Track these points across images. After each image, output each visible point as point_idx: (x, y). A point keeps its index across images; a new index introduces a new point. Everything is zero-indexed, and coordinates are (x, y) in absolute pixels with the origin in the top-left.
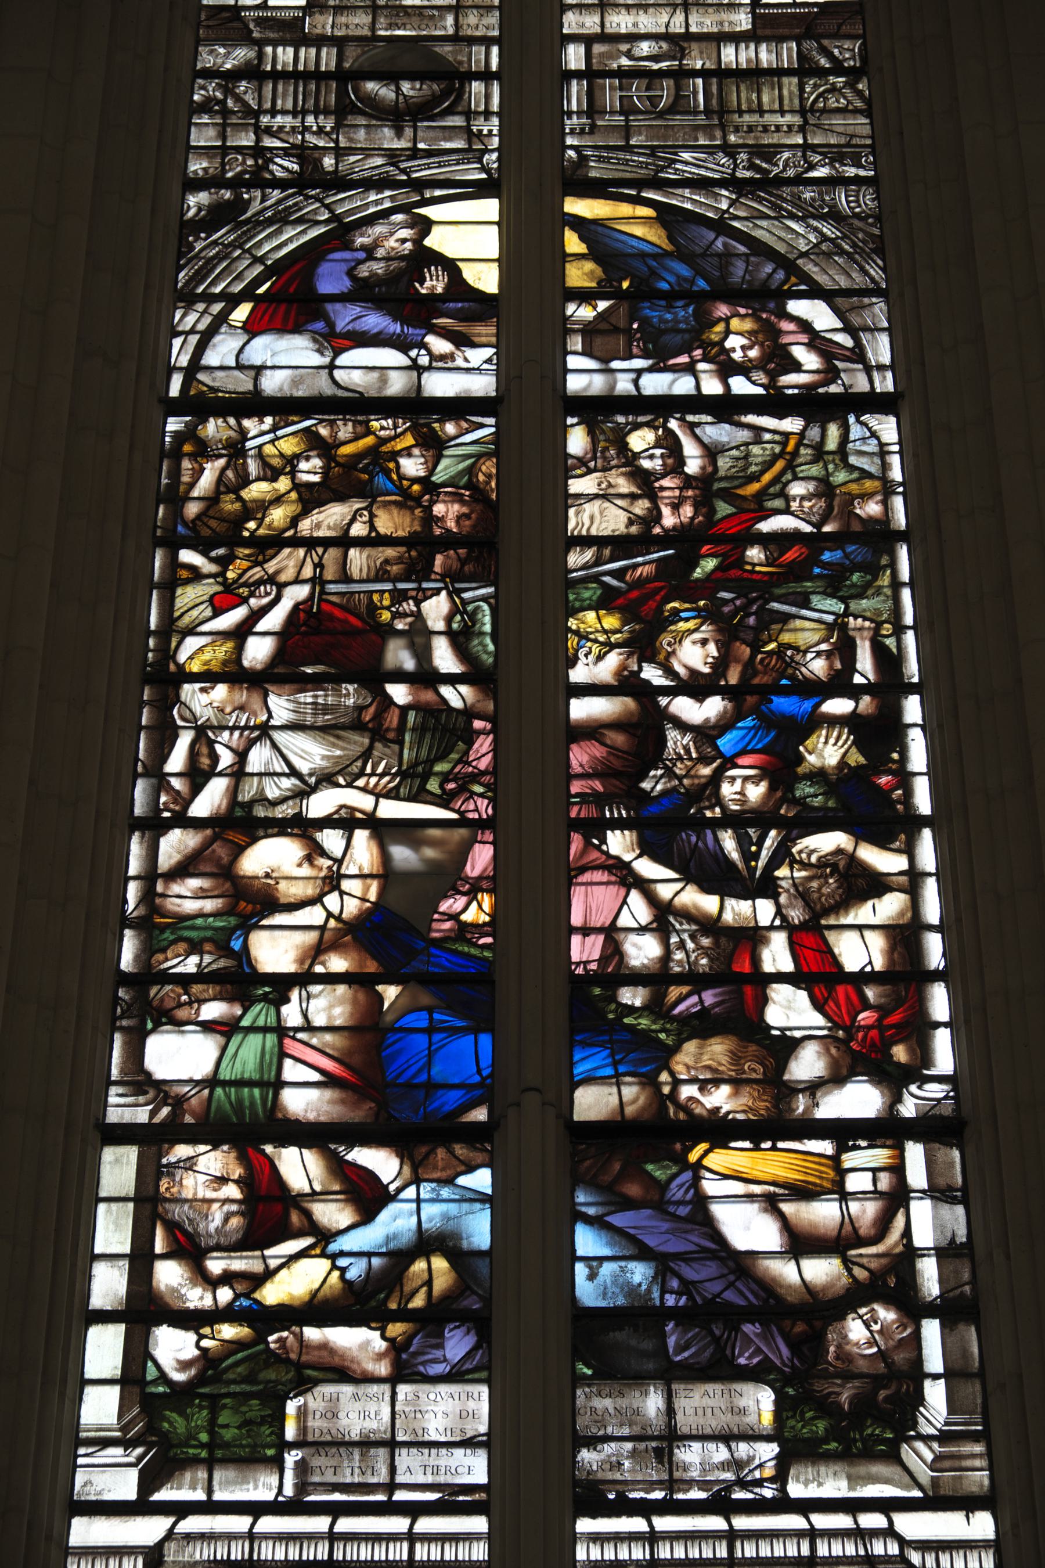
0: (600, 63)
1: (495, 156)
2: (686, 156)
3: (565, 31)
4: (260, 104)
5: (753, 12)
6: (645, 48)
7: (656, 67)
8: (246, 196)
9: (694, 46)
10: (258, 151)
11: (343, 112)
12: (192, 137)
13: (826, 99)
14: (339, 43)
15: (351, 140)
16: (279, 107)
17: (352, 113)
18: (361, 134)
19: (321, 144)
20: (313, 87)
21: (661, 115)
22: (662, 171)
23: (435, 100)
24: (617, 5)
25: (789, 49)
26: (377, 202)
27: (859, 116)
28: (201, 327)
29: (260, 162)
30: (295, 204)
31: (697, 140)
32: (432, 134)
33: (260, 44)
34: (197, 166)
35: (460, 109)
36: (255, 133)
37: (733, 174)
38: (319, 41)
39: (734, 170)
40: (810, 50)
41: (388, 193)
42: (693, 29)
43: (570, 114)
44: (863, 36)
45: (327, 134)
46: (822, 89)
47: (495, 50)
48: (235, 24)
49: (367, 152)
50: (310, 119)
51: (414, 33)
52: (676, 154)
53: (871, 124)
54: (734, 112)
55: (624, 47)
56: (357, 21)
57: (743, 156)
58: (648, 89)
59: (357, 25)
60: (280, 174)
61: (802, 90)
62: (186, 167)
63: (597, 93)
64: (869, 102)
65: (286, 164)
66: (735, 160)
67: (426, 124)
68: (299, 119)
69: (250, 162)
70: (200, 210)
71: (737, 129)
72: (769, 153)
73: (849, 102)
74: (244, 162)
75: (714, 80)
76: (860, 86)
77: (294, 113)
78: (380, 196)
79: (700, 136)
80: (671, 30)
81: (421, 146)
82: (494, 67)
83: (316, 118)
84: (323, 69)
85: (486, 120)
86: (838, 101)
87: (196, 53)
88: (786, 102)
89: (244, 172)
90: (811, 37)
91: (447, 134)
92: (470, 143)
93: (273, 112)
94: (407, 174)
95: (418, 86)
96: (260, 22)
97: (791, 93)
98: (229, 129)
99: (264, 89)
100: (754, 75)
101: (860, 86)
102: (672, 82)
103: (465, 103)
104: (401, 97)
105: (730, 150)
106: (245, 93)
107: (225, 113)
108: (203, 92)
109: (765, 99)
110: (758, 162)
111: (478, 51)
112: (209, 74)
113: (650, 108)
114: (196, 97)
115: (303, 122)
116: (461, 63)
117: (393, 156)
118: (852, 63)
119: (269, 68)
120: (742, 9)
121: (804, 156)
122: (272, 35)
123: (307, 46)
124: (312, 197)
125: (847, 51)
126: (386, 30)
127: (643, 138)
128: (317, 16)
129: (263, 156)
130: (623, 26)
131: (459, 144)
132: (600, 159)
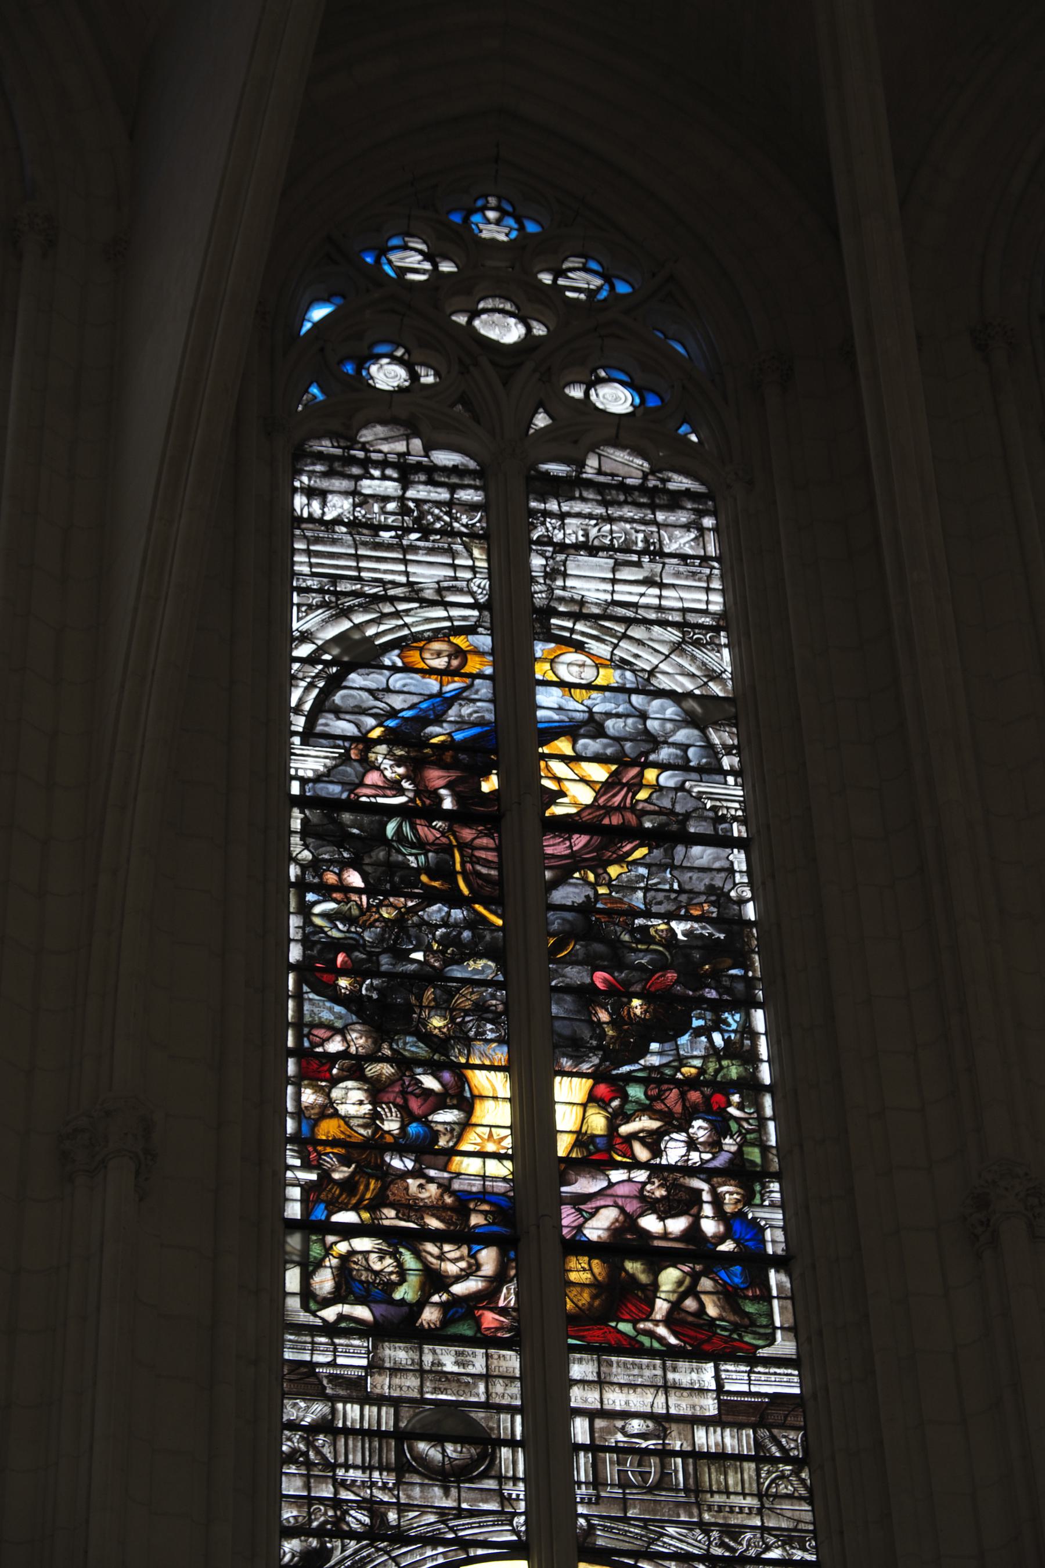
0: (601, 1437)
1: (522, 1519)
2: (671, 1530)
3: (572, 1405)
4: (335, 1458)
5: (718, 1398)
6: (636, 1425)
7: (644, 1444)
8: (329, 1545)
9: (674, 1426)
10: (336, 1503)
11: (401, 1469)
12: (284, 1486)
13: (777, 1485)
14: (395, 1402)
15: (409, 1497)
16: (350, 1462)
17: (410, 1472)
18: (417, 1491)
19: (386, 1499)
20: (376, 1444)
21: (650, 1490)
22: (652, 1543)
23: (475, 1463)
24: (612, 1384)
25: (748, 1436)
26: (433, 1558)
27: (803, 1503)
29: (339, 1513)
30: (369, 1555)
31: (679, 1516)
32: (472, 1495)
33: (332, 1400)
34: (289, 1514)
35: (493, 1473)
36: (334, 1486)
37: (708, 1550)
38: (380, 1401)
39: (709, 1546)
40: (764, 1438)
41: (441, 1550)
42: (672, 1411)
43: (579, 1483)
44: (804, 1428)
45: (391, 1490)
46: (774, 1475)
47: (518, 1419)
48: (312, 1380)
49: (423, 1509)
50: (376, 1474)
51: (454, 1398)
52: (663, 1528)
53: (813, 1511)
54: (707, 1492)
55: (619, 1424)
56: (408, 1384)
57: (715, 1534)
58: (639, 1465)
59: (409, 1387)
60: (355, 1526)
61: (758, 1476)
62: (280, 1515)
63: (600, 1466)
64: (810, 1490)
65: (359, 1516)
66: (709, 1537)
67: (467, 1485)
68: (367, 1475)
69: (330, 1513)
70: (293, 1556)
71: (710, 1509)
72: (733, 1532)
73: (795, 1489)
74: (325, 1514)
75: (691, 1461)
76: (803, 1475)
77: (363, 1468)
78: (435, 1552)
79: (681, 1512)
80: (655, 1410)
81: (464, 1506)
82: (518, 1438)
83: (381, 1474)
84: (383, 1428)
85: (514, 1485)
86: (786, 1488)
87: (282, 1406)
88: (747, 1485)
89: (326, 1522)
90: (764, 1426)
91: (484, 1496)
92: (502, 1506)
93: (347, 1467)
94: (455, 1532)
95: (459, 1449)
96: (332, 1378)
97: (750, 1477)
98: (312, 1481)
99: (338, 1443)
100: (721, 1458)
101: (803, 1475)
102: (657, 1460)
103: (496, 1468)
104: (446, 1459)
105: (705, 1528)
106: (323, 1446)
107: (309, 1464)
108: (289, 1443)
109: (731, 1481)
110: (727, 1540)
111: (505, 1418)
112: (294, 1426)
113: (641, 1483)
114: (285, 1448)
115: (370, 1478)
116: (492, 1429)
117: (443, 1513)
118: (796, 1453)
119: (340, 1425)
120: (710, 1394)
121: (762, 1537)
122: (342, 1393)
123: (371, 1405)
124: (381, 1549)
125: (792, 1440)
126: (432, 1393)
127: (636, 1511)
128: (376, 1376)
129: (341, 1508)
130: (617, 1403)
131: (493, 1506)
132: (605, 1529)
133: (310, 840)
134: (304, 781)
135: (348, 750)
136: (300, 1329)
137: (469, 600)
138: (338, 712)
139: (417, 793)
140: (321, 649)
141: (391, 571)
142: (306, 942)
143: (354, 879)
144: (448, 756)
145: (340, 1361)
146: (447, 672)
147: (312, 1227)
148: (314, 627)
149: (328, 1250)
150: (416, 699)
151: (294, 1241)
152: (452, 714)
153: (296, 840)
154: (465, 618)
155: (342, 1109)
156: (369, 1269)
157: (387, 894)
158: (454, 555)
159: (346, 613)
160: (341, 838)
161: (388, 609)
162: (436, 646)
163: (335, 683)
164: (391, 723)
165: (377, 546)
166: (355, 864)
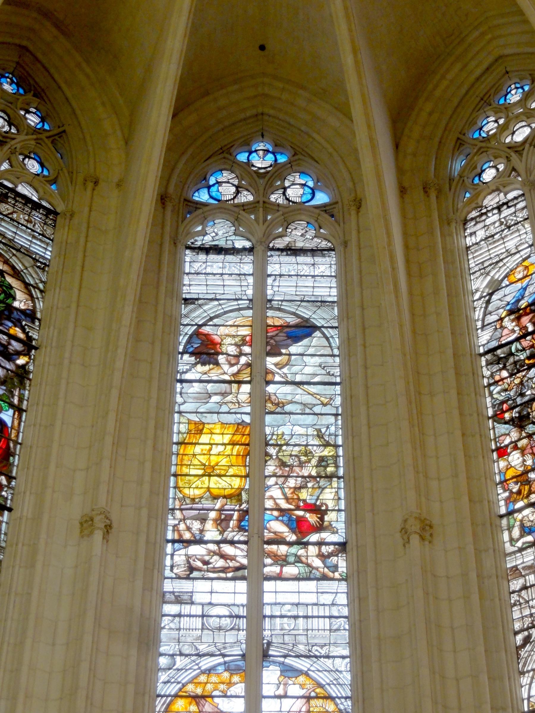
28: (528, 682)
34: (517, 626)
96: (524, 568)
107: (520, 604)
133: (489, 367)
134: (484, 345)
135: (496, 326)
136: (510, 554)
137: (527, 245)
138: (490, 313)
139: (520, 330)
140: (483, 292)
141: (499, 249)
142: (493, 406)
143: (505, 374)
144: (528, 310)
145: (525, 560)
146: (525, 277)
147: (510, 513)
148: (479, 284)
149: (515, 520)
150: (514, 294)
151: (504, 521)
152: (527, 293)
153: (484, 369)
154: (526, 253)
155: (513, 465)
156: (530, 521)
157: (515, 374)
158: (518, 230)
159: (488, 274)
160: (499, 360)
161: (501, 264)
162: (518, 269)
163: (488, 302)
164: (508, 308)
165: (494, 242)
166: (504, 368)
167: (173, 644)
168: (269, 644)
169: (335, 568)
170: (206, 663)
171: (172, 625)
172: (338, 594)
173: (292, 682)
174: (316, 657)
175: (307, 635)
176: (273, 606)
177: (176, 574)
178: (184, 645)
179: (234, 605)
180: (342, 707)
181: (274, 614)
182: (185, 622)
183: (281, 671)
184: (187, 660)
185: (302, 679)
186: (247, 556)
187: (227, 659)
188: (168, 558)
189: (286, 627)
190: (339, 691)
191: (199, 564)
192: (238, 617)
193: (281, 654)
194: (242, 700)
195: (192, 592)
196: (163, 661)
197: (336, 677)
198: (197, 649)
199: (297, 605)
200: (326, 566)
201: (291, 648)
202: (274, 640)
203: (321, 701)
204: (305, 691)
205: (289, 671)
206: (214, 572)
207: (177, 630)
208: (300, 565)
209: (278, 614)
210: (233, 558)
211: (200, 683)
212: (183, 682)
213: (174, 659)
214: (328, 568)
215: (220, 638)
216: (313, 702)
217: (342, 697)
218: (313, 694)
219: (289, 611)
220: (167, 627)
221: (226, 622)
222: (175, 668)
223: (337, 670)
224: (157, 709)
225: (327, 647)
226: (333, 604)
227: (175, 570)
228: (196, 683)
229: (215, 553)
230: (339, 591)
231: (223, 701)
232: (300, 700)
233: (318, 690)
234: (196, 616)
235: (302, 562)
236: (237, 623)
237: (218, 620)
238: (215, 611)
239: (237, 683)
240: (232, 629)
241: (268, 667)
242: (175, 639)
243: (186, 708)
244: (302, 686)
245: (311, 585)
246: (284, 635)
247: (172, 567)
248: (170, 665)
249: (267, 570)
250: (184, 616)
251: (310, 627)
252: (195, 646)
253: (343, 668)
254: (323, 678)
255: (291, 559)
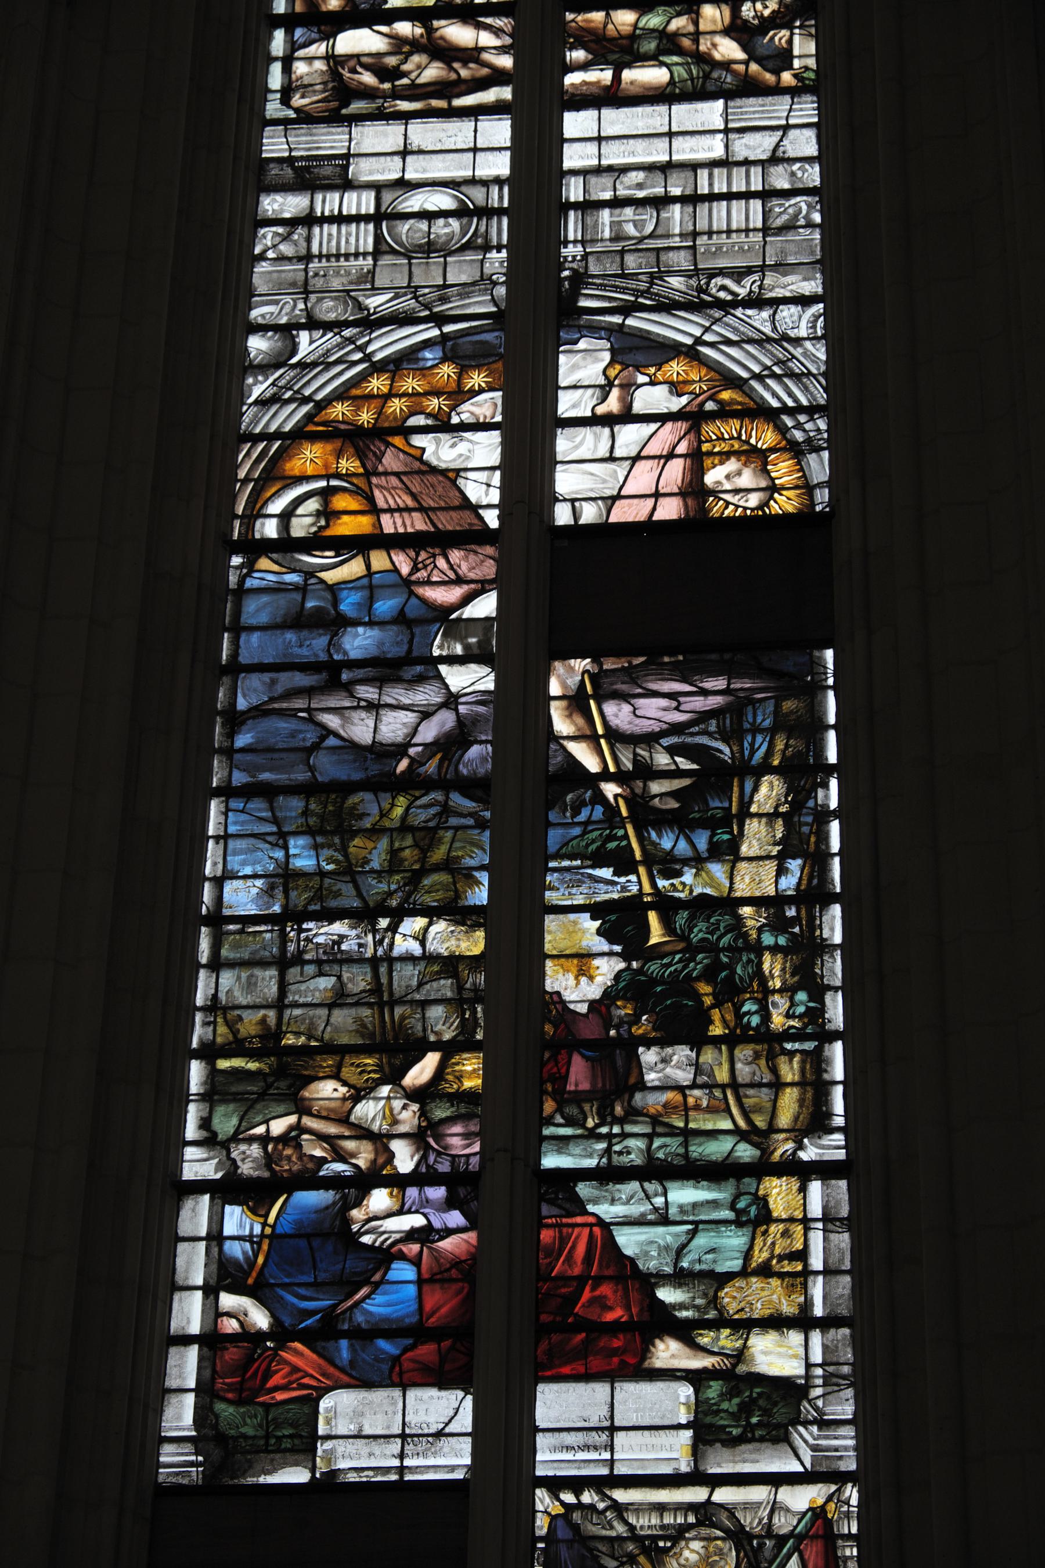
167: (288, 298)
168: (580, 279)
169: (783, 58)
170: (386, 343)
171: (286, 249)
172: (793, 134)
173: (646, 379)
174: (720, 304)
175: (693, 248)
176: (593, 180)
177: (297, 110)
178: (320, 300)
179: (473, 181)
180: (799, 435)
181: (594, 197)
182: (323, 238)
183: (612, 350)
184: (330, 339)
185: (675, 368)
186: (511, 46)
187: (448, 329)
188: (276, 69)
189: (630, 230)
190: (790, 394)
191: (368, 78)
192: (486, 212)
193: (614, 304)
194: (494, 437)
195: (347, 156)
196: (258, 345)
197: (780, 354)
198: (360, 307)
199: (666, 168)
200: (752, 56)
201: (643, 286)
202: (594, 269)
203: (735, 424)
204: (684, 400)
205: (638, 348)
206: (410, 99)
207: (300, 259)
208: (675, 59)
209: (607, 195)
210: (472, 55)
211: (370, 397)
212: (319, 396)
213: (293, 337)
214: (758, 62)
215: (428, 275)
216: (710, 430)
217: (800, 409)
218: (710, 406)
219: (640, 186)
220: (271, 254)
221: (447, 230)
222: (294, 361)
223: (785, 338)
224: (242, 474)
225: (756, 277)
226: (775, 159)
227: (297, 101)
228: (355, 398)
229: (413, 46)
230: (792, 121)
231: (438, 442)
232: (669, 425)
233: (725, 395)
234: (358, 219)
235: (680, 51)
236: (483, 229)
237: (424, 226)
238: (415, 202)
239: (481, 391)
240: (464, 248)
241: (576, 342)
242: (293, 284)
243: (326, 466)
244: (676, 388)
245: (711, 113)
246: (622, 252)
247: (286, 94)
248: (280, 354)
249: (572, 79)
250: (323, 220)
251: (702, 225)
252: (355, 299)
253: (803, 332)
254: (742, 361)
255: (651, 46)
